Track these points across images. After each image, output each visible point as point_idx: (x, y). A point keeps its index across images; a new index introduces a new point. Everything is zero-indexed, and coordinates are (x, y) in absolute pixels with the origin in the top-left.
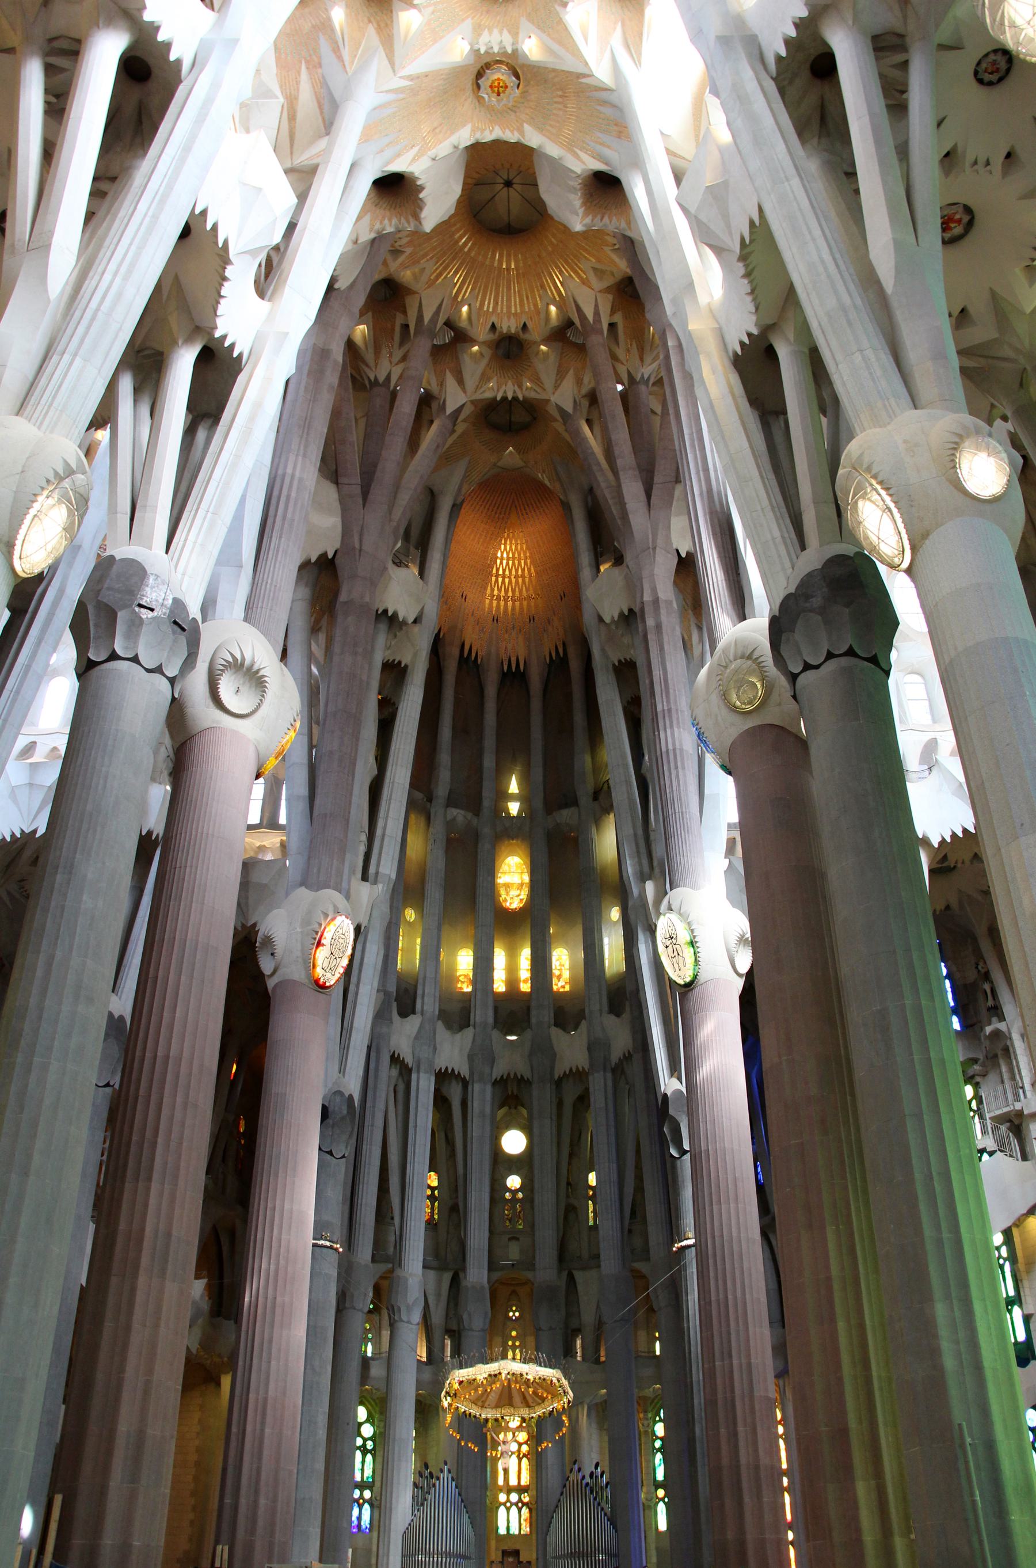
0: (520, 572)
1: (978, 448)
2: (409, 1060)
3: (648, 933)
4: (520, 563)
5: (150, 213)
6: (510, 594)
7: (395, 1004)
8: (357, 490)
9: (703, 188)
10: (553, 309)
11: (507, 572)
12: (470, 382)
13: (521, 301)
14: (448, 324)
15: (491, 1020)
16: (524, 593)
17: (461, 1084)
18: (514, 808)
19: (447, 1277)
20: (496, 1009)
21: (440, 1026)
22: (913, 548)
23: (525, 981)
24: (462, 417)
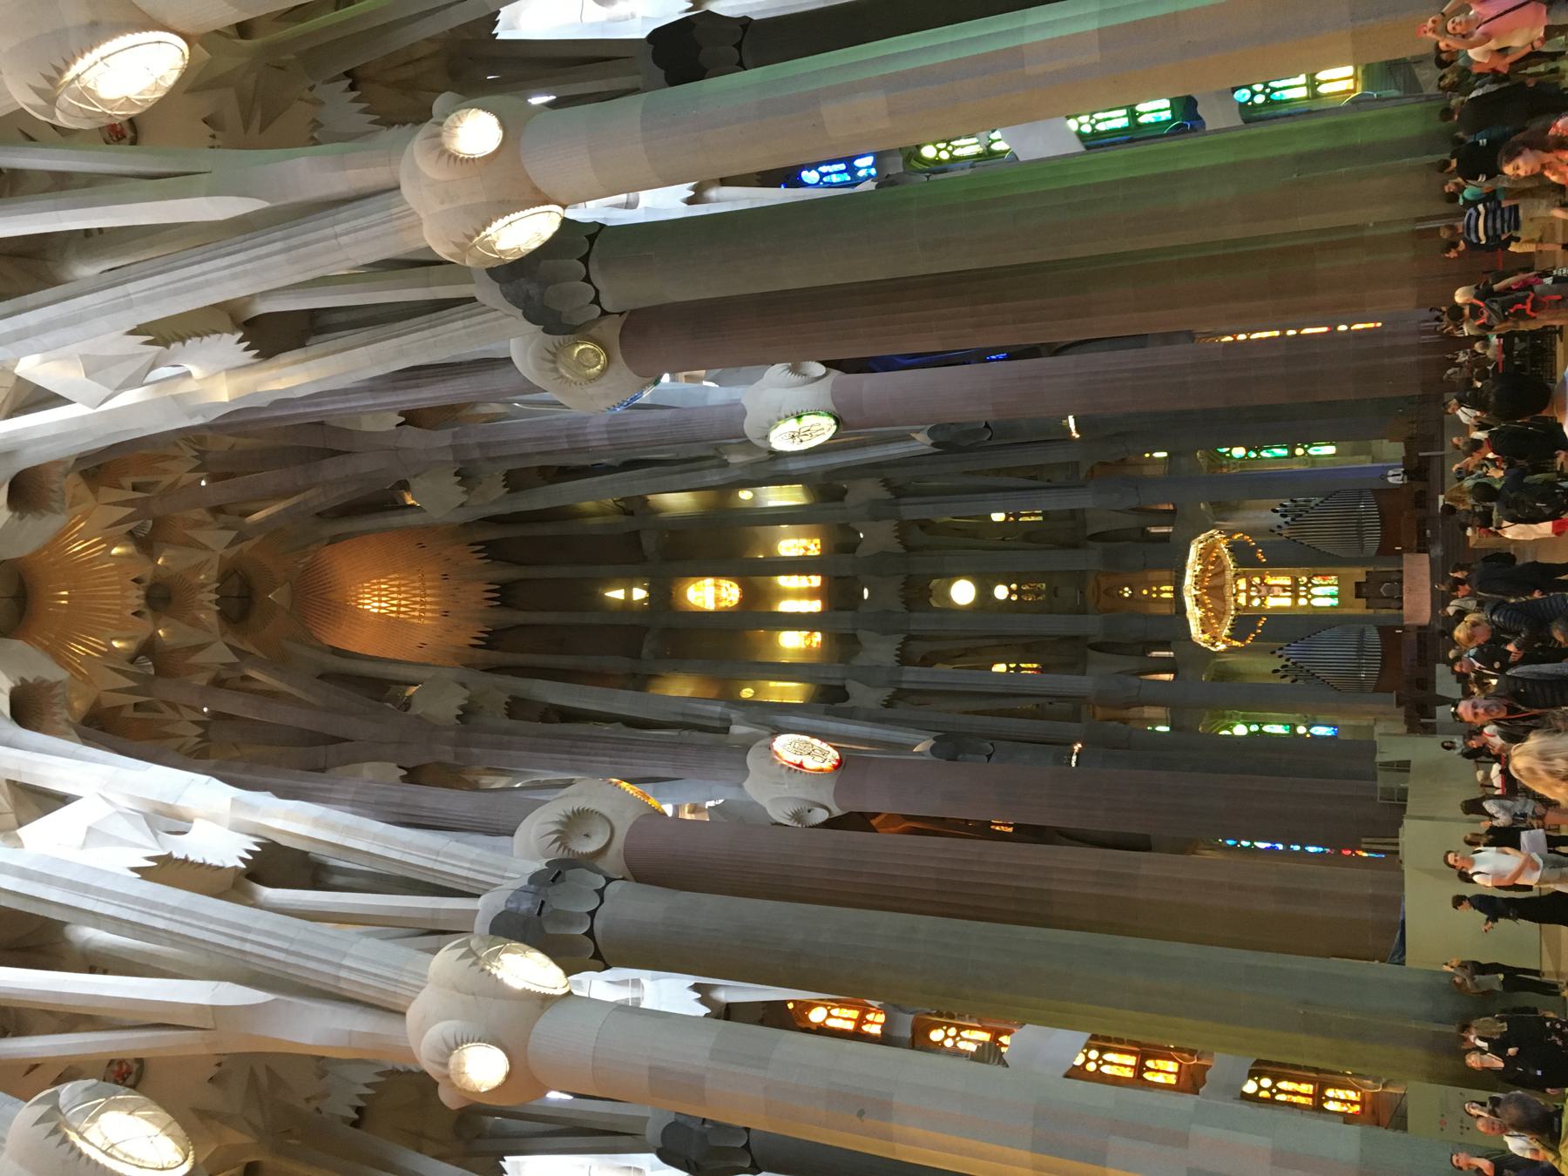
0: (395, 589)
1: (453, 136)
2: (889, 691)
3: (778, 461)
4: (385, 589)
5: (168, 916)
6: (418, 599)
7: (837, 705)
8: (332, 748)
9: (89, 381)
10: (116, 551)
11: (395, 602)
12: (198, 638)
13: (107, 584)
14: (132, 661)
15: (849, 614)
16: (417, 584)
17: (911, 642)
18: (639, 594)
19: (1093, 654)
20: (838, 609)
21: (857, 662)
22: (547, 202)
23: (810, 581)
24: (238, 645)
